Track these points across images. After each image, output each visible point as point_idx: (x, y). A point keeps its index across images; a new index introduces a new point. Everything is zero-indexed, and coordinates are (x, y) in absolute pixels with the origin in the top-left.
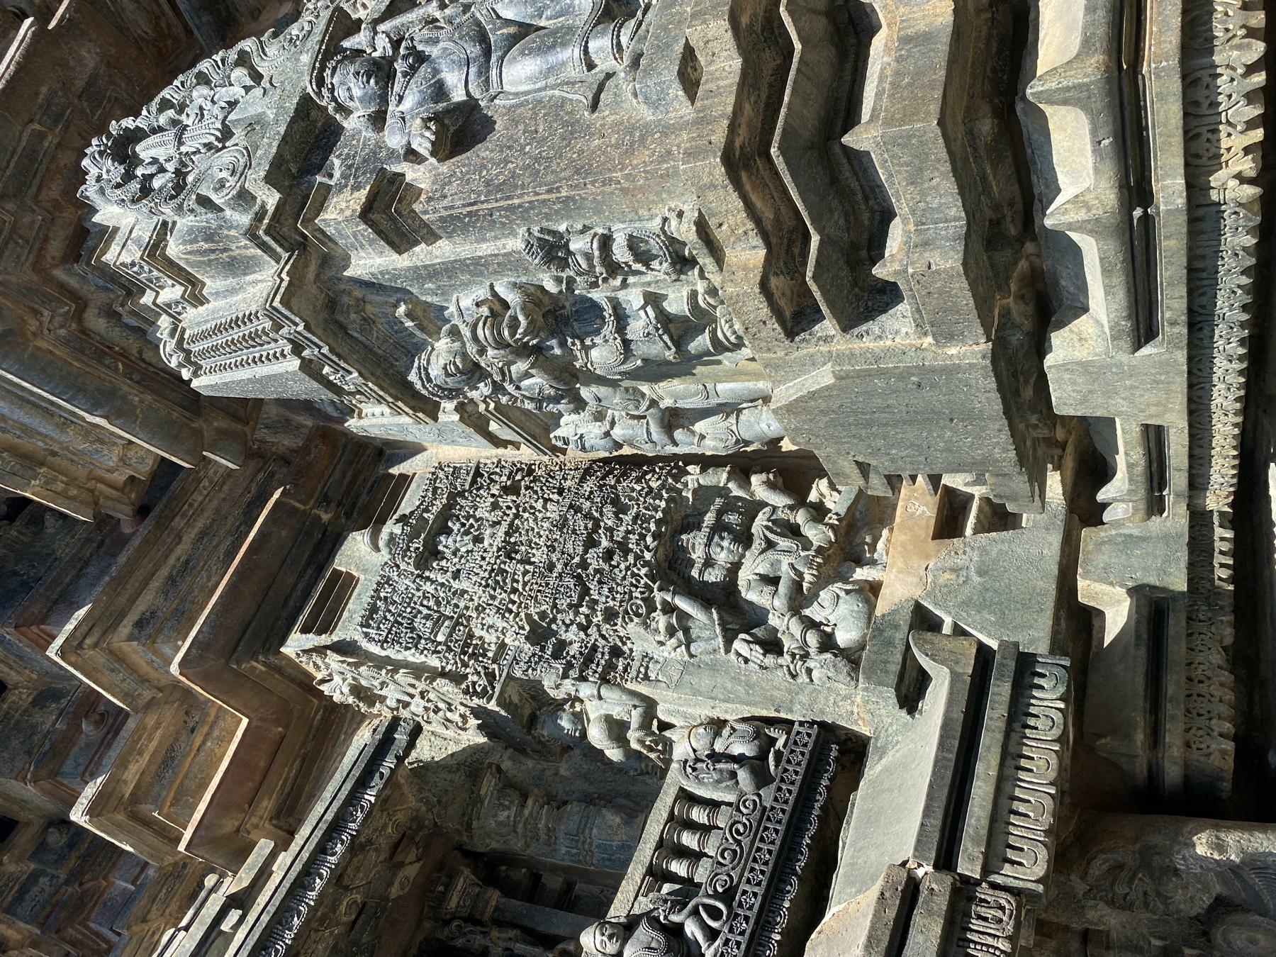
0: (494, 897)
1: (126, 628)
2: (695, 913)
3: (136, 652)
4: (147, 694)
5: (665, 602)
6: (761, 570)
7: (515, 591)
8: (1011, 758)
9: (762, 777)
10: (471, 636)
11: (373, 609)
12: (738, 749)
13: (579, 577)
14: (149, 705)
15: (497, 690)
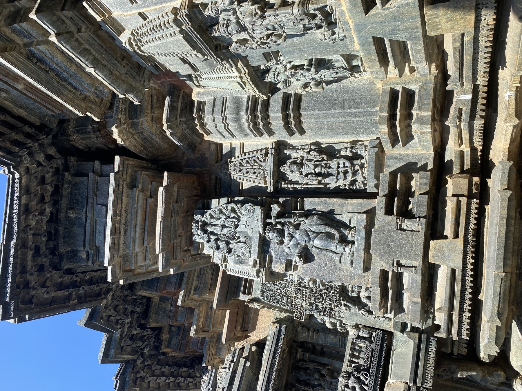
0: (307, 355)
1: (192, 293)
2: (362, 374)
3: (196, 297)
4: (198, 303)
5: (344, 304)
6: (366, 295)
7: (303, 295)
8: (426, 361)
9: (371, 342)
10: (292, 302)
11: (263, 292)
12: (365, 335)
13: (320, 294)
14: (199, 305)
15: (304, 317)
